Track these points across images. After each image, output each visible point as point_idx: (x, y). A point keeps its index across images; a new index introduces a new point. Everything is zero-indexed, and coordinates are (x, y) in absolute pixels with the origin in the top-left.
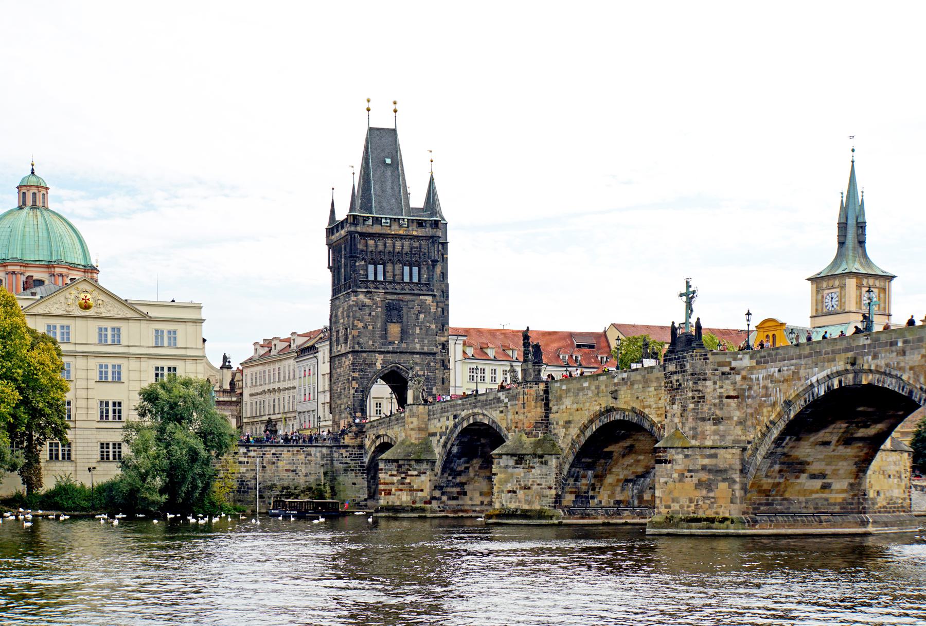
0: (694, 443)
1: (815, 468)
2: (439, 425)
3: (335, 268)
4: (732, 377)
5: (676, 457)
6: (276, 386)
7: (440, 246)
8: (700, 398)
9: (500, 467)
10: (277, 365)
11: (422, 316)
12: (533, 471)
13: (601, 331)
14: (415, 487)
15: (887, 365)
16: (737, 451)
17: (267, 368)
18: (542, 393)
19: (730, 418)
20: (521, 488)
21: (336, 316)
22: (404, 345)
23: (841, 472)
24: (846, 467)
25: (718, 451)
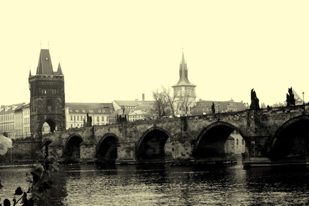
0: (125, 142)
1: (152, 146)
2: (65, 136)
3: (31, 90)
4: (133, 127)
5: (121, 145)
6: (7, 121)
7: (62, 83)
8: (126, 132)
9: (82, 148)
10: (7, 115)
11: (57, 103)
12: (90, 149)
13: (111, 102)
14: (58, 153)
15: (161, 126)
16: (134, 144)
17: (4, 115)
18: (92, 129)
19: (133, 136)
20: (87, 153)
21: (32, 103)
22: (52, 112)
23: (158, 147)
24: (158, 146)
25: (130, 144)
